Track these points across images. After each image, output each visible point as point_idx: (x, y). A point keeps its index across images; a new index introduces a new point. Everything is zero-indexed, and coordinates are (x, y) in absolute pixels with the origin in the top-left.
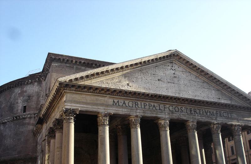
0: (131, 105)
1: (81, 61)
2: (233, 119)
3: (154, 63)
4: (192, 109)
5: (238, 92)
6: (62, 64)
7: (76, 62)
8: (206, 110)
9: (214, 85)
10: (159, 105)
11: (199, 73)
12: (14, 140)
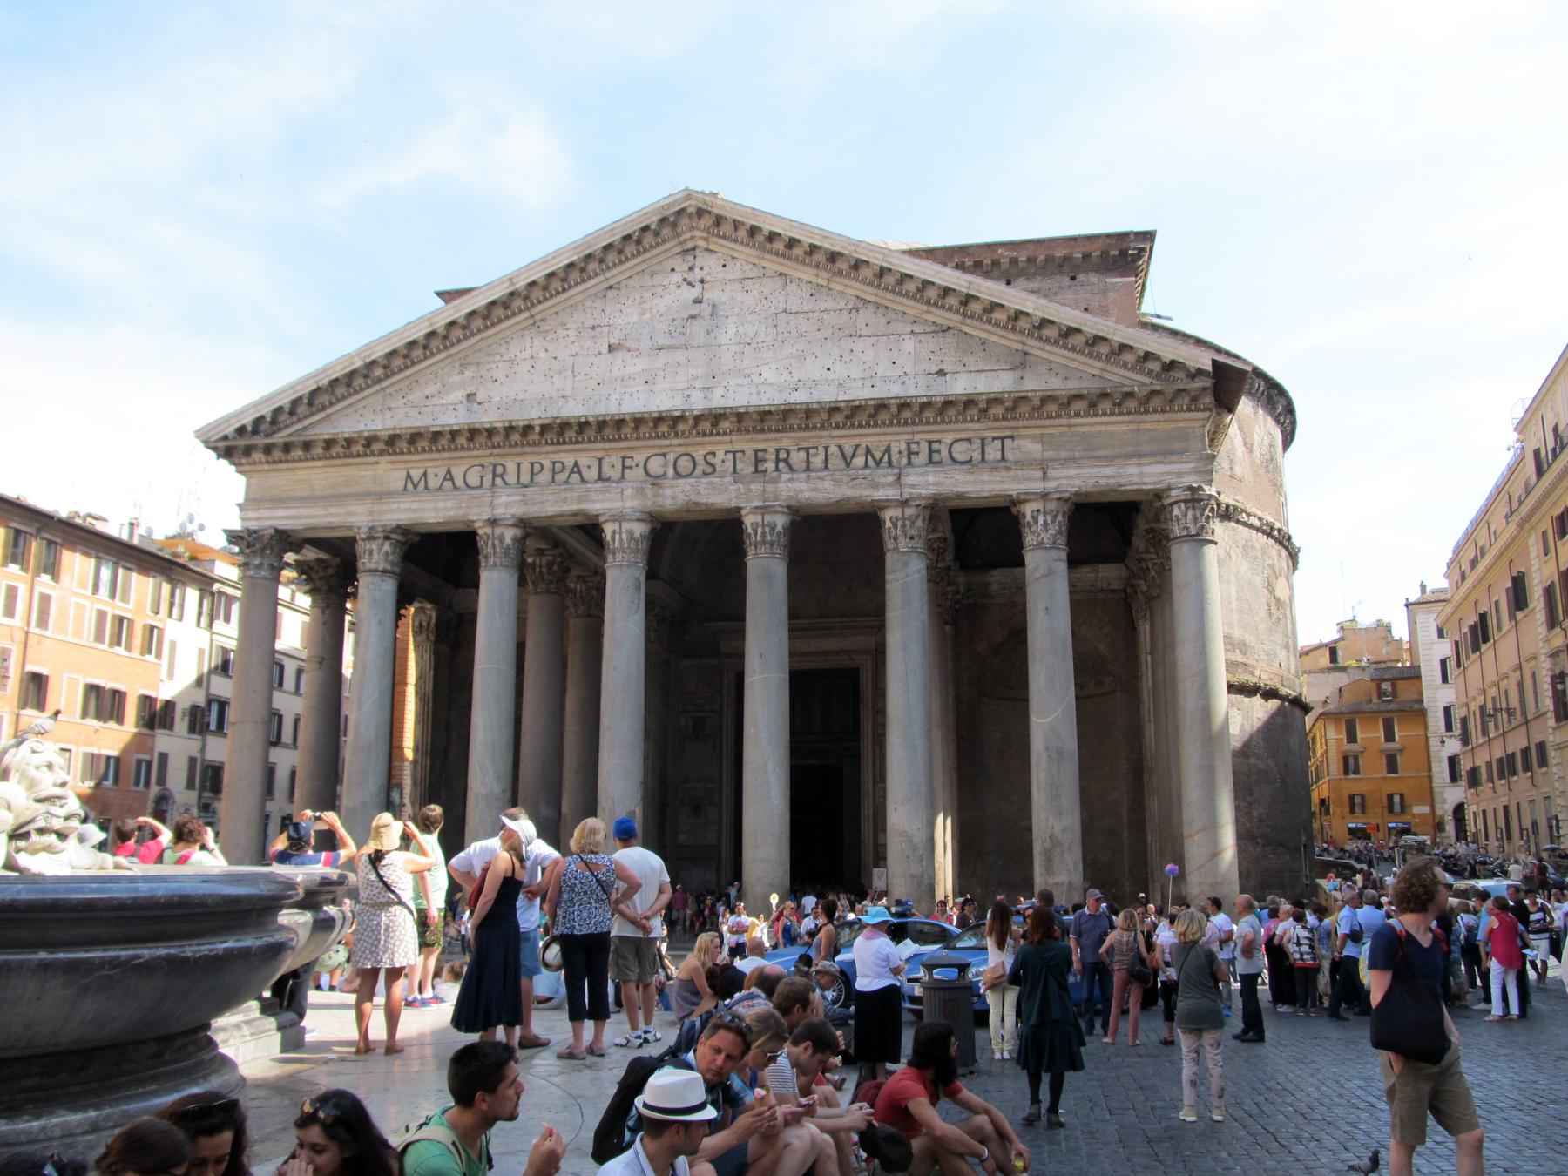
0: (473, 480)
2: (1007, 469)
3: (590, 278)
4: (765, 451)
8: (848, 450)
9: (913, 308)
10: (600, 460)
11: (825, 269)
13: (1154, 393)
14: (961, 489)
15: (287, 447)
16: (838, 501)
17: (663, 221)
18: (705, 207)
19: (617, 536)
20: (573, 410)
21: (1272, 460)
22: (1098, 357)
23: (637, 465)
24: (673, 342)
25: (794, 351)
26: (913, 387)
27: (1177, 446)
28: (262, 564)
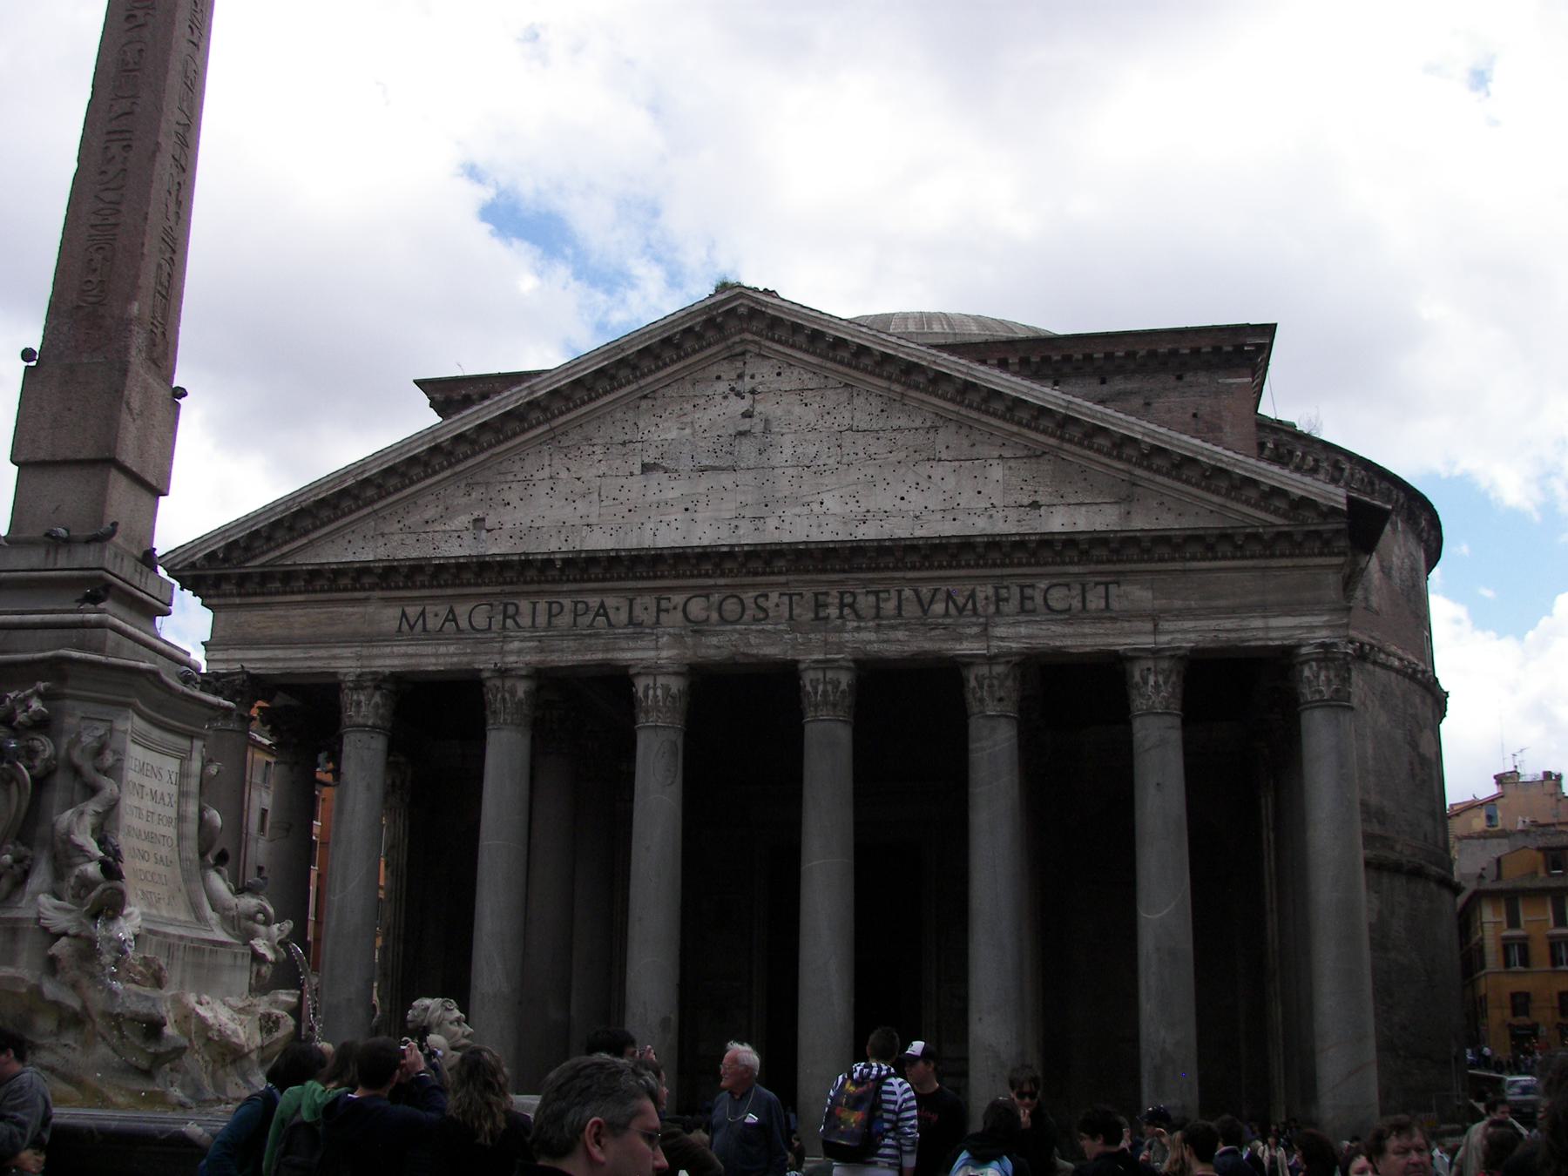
0: (480, 620)
2: (1114, 619)
3: (621, 386)
4: (826, 594)
8: (925, 591)
10: (631, 602)
11: (898, 382)
13: (1279, 535)
14: (1058, 644)
15: (265, 578)
16: (913, 655)
17: (706, 322)
18: (758, 307)
19: (651, 692)
20: (599, 541)
21: (1414, 586)
22: (1216, 492)
23: (675, 608)
24: (717, 464)
25: (862, 477)
26: (1001, 521)
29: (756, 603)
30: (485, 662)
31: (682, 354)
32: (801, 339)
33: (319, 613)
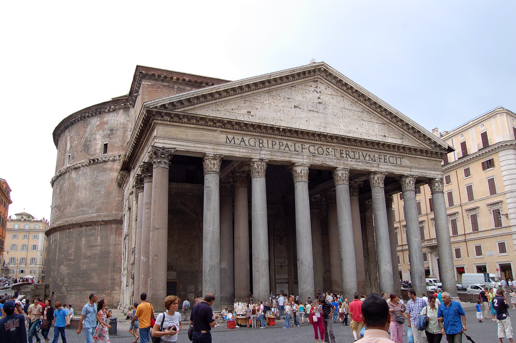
1: (185, 78)
3: (289, 82)
4: (343, 150)
5: (413, 128)
6: (157, 83)
7: (178, 79)
10: (295, 144)
11: (356, 98)
12: (92, 192)
18: (327, 69)
27: (436, 167)
28: (167, 163)
29: (326, 150)
30: (256, 156)
31: (304, 77)
32: (334, 81)
33: (198, 132)
